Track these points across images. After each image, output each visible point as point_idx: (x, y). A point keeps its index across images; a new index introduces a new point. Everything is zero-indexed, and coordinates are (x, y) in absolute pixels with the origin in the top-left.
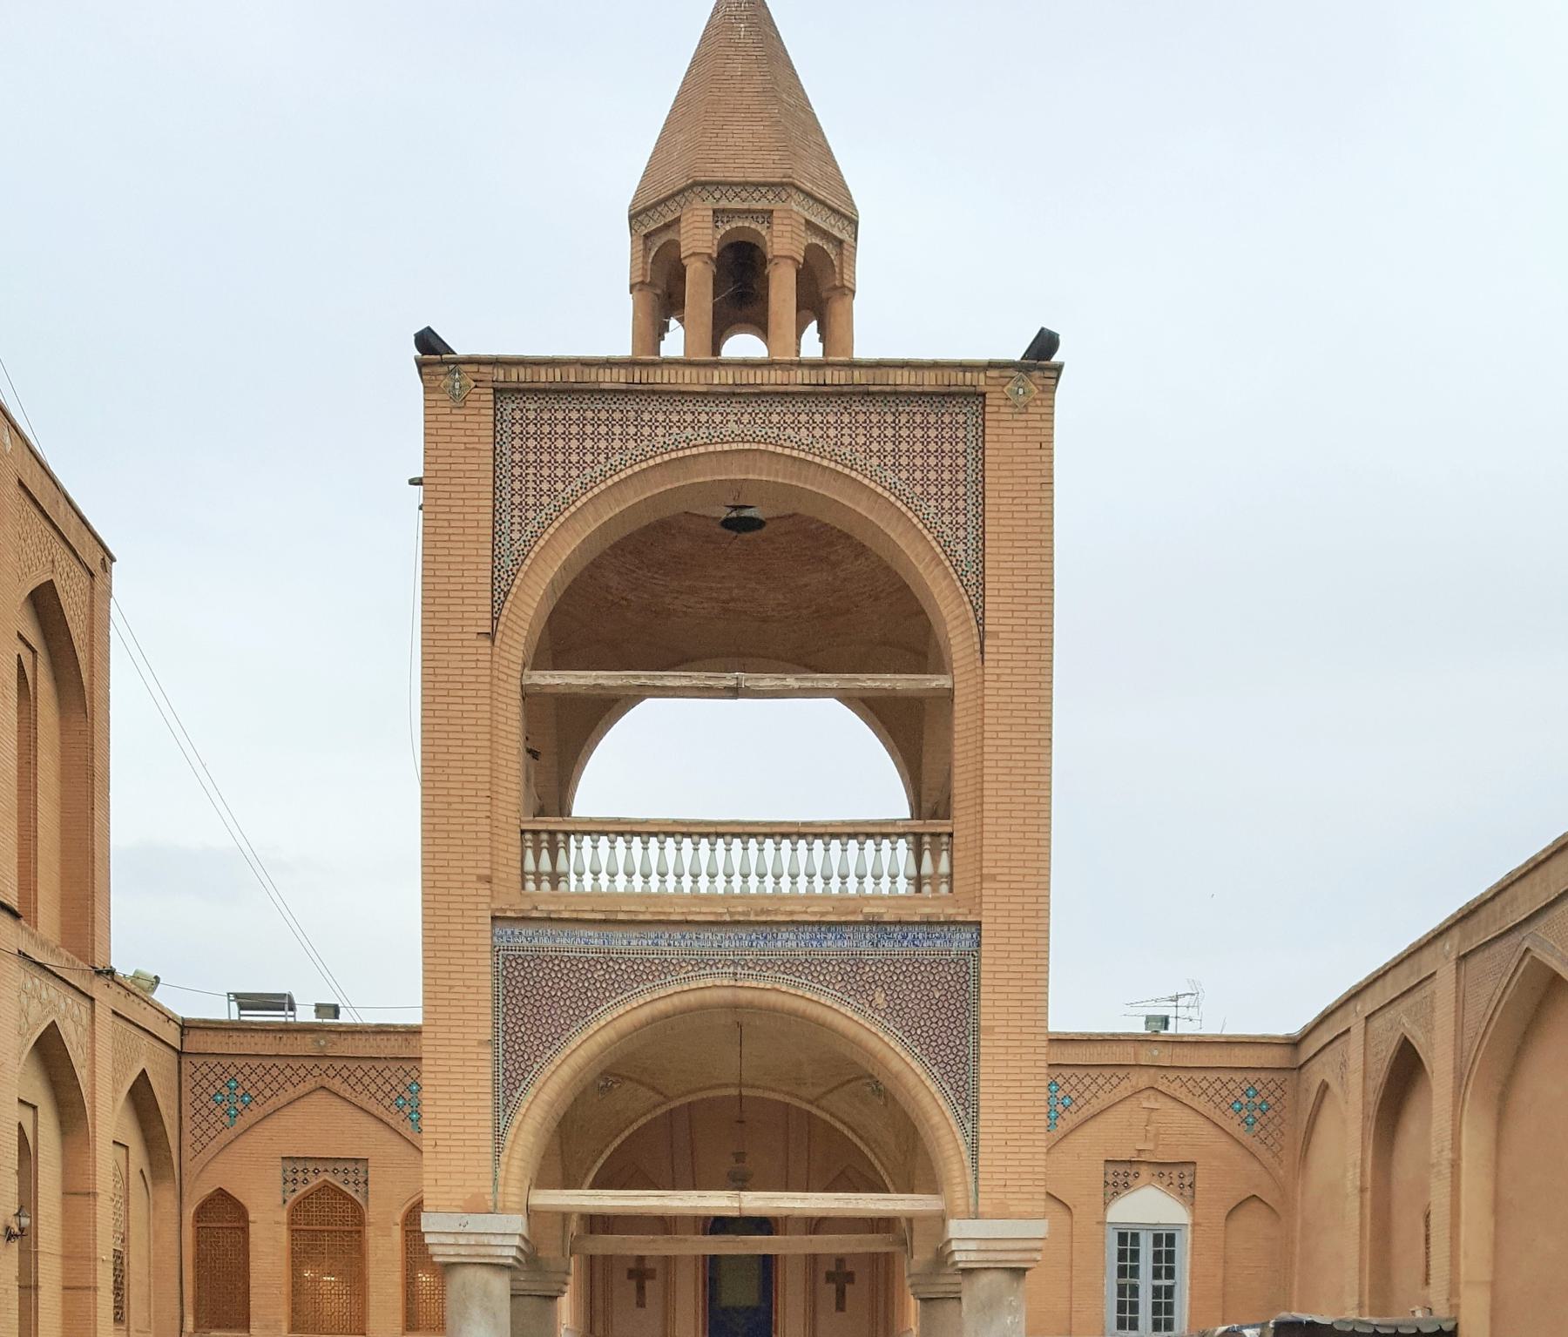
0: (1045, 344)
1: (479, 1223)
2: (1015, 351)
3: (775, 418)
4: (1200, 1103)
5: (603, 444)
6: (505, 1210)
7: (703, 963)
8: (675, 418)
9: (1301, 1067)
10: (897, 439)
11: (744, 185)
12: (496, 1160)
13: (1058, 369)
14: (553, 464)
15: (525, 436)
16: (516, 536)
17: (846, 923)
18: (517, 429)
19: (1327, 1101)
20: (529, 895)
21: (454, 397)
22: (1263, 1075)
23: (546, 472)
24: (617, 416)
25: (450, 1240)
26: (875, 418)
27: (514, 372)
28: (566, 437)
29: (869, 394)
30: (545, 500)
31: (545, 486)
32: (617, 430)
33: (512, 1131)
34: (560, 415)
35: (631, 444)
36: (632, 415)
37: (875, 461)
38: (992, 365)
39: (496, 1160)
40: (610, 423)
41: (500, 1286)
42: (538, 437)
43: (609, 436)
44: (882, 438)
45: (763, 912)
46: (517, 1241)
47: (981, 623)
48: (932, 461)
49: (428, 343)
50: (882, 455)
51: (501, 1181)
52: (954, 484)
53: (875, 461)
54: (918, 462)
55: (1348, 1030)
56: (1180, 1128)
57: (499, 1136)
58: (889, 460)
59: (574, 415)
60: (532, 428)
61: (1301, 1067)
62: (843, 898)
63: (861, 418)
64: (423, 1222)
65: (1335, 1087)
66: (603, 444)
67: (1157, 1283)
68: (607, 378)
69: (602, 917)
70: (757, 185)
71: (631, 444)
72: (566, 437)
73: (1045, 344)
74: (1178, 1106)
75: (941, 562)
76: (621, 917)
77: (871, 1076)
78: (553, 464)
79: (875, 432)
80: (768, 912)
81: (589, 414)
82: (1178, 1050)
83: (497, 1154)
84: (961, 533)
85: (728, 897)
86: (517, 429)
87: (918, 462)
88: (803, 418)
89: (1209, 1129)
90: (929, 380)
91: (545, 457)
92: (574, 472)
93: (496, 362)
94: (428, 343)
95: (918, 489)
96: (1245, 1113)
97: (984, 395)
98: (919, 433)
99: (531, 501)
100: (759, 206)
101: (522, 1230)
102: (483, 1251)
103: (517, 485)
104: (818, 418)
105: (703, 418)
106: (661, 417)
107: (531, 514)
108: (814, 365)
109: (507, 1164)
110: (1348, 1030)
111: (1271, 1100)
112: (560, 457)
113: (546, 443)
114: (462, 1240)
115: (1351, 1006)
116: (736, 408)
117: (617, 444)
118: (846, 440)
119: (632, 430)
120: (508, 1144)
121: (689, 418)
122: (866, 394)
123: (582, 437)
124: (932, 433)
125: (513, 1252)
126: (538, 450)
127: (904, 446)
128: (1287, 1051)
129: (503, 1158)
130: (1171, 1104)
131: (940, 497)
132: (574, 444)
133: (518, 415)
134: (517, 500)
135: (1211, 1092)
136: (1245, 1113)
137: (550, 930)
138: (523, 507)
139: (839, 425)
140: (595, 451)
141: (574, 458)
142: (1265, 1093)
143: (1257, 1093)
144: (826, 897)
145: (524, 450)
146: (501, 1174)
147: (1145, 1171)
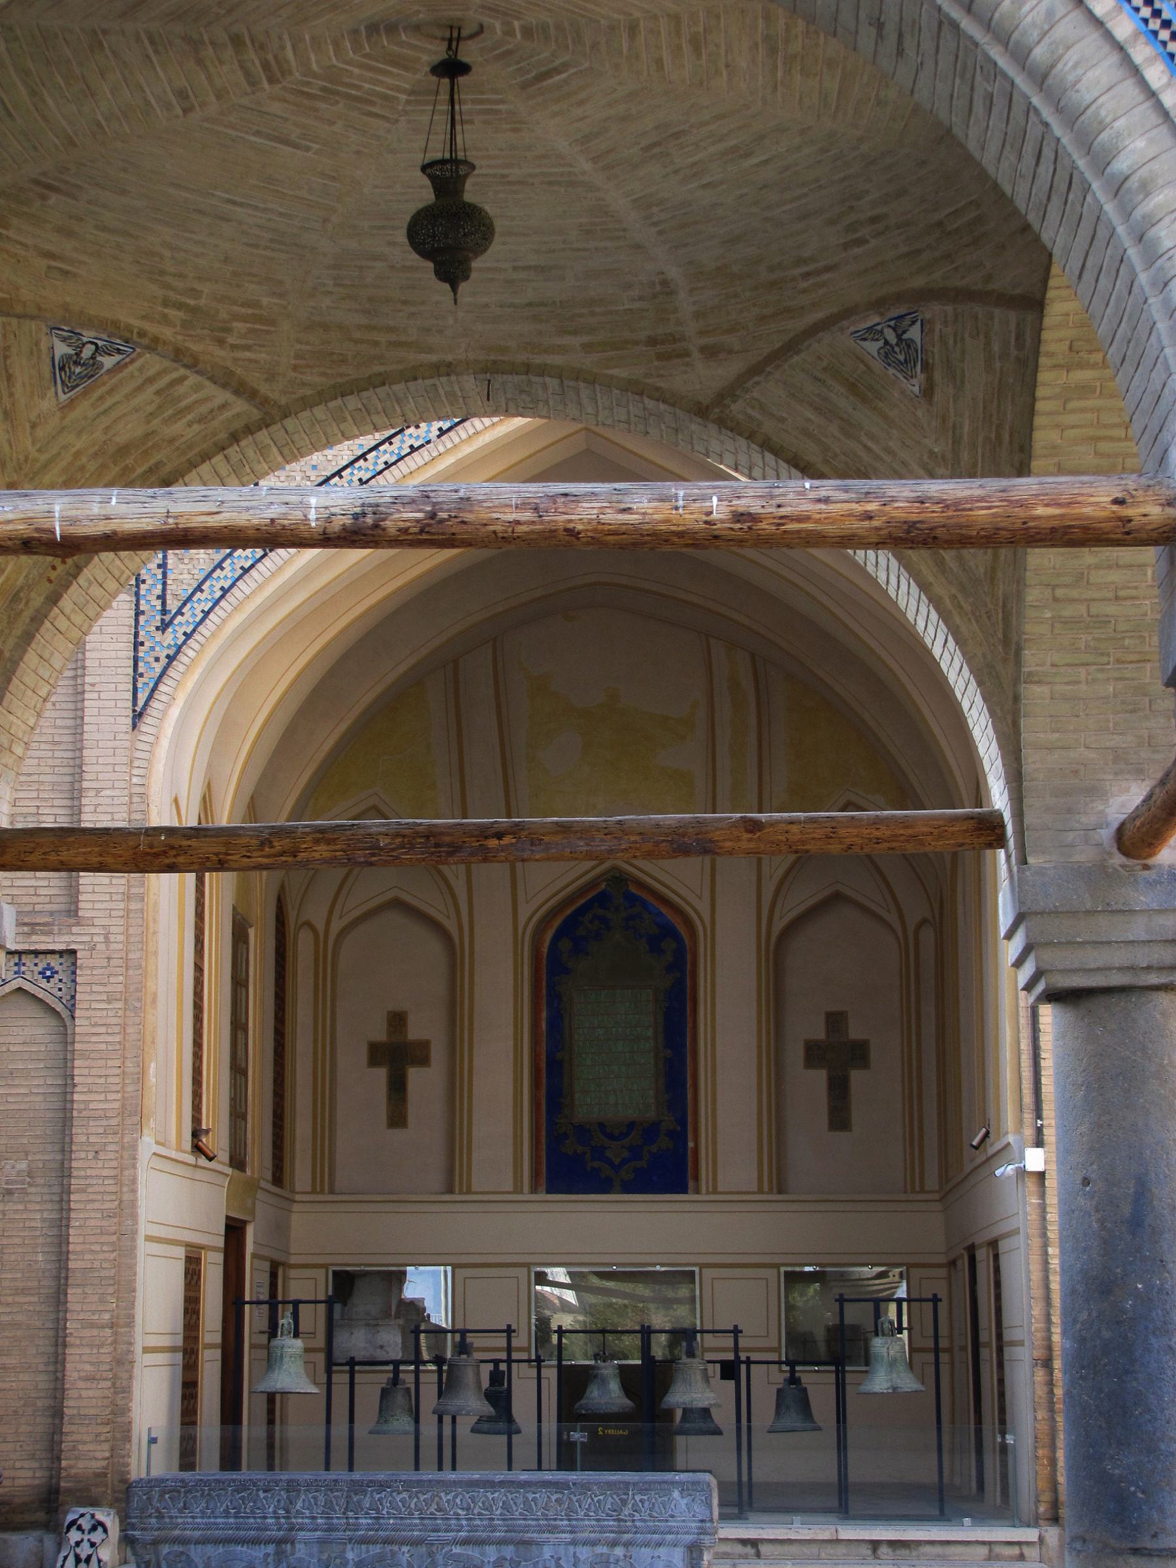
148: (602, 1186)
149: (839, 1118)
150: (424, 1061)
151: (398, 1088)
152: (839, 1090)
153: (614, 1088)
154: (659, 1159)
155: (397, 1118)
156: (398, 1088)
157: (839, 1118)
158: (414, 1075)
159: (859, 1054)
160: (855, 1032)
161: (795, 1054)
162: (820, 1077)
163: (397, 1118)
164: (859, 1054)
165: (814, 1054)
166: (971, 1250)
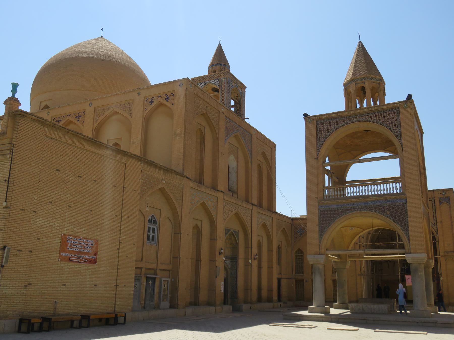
0: (410, 97)
2: (404, 99)
6: (322, 254)
10: (384, 117)
28: (328, 126)
38: (400, 102)
39: (320, 245)
43: (335, 124)
47: (402, 145)
49: (305, 115)
50: (381, 120)
52: (395, 123)
57: (320, 241)
93: (316, 116)
94: (305, 115)
108: (365, 108)
131: (392, 126)
138: (321, 138)
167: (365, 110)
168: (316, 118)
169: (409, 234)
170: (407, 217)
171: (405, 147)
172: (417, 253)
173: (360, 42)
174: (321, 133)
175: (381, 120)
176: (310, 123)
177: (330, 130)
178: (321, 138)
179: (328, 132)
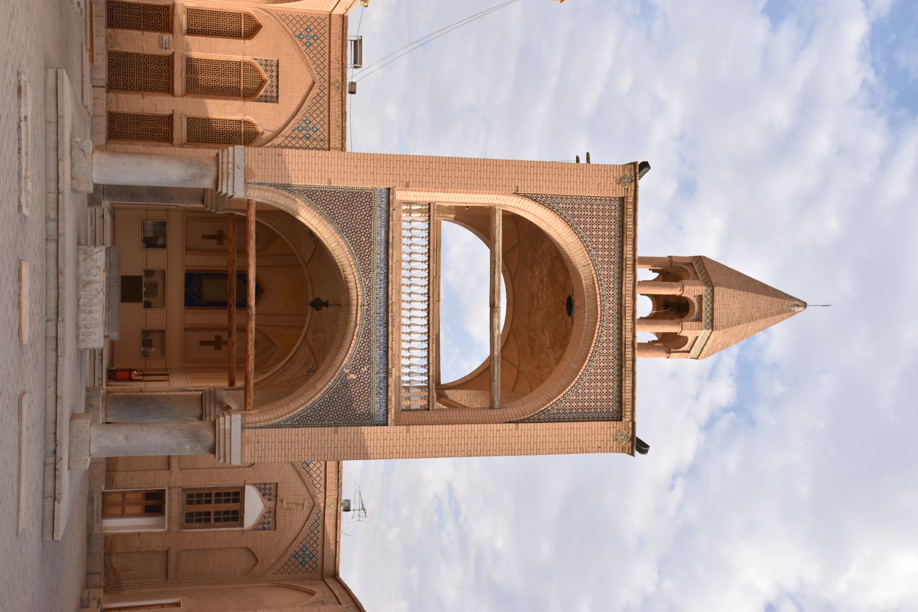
0: (641, 447)
1: (239, 174)
3: (611, 325)
4: (306, 530)
5: (600, 246)
6: (246, 188)
7: (369, 290)
8: (611, 279)
9: (323, 580)
10: (602, 381)
11: (712, 309)
12: (271, 185)
13: (633, 454)
14: (592, 223)
15: (604, 210)
16: (561, 205)
17: (387, 360)
18: (607, 207)
19: (304, 595)
20: (400, 206)
21: (621, 179)
22: (320, 558)
23: (588, 220)
24: (612, 253)
25: (230, 160)
26: (611, 371)
27: (632, 207)
28: (604, 230)
29: (621, 368)
30: (576, 219)
31: (582, 219)
32: (606, 253)
33: (287, 194)
34: (613, 227)
35: (600, 259)
36: (613, 260)
37: (593, 371)
39: (271, 185)
40: (609, 250)
41: (208, 183)
42: (604, 217)
43: (603, 249)
44: (602, 374)
45: (393, 319)
46: (230, 194)
47: (523, 421)
48: (593, 397)
49: (645, 166)
50: (596, 374)
51: (261, 187)
53: (593, 371)
54: (592, 391)
55: (340, 604)
56: (293, 521)
58: (593, 378)
59: (613, 234)
60: (607, 214)
61: (323, 580)
62: (399, 357)
63: (611, 364)
64: (240, 146)
65: (313, 599)
66: (600, 246)
67: (212, 514)
68: (628, 249)
69: (390, 241)
70: (712, 315)
71: (600, 259)
72: (604, 230)
73: (641, 447)
74: (305, 519)
75: (549, 402)
76: (390, 250)
77: (317, 368)
78: (592, 223)
79: (605, 371)
80: (392, 322)
81: (613, 240)
82: (334, 517)
83: (275, 186)
84: (561, 411)
85: (400, 301)
86: (607, 207)
87: (592, 391)
88: (611, 338)
89: (293, 535)
90: (627, 396)
91: (594, 220)
92: (588, 233)
94: (645, 166)
95: (580, 391)
96: (301, 553)
97: (621, 420)
98: (605, 391)
99: (576, 213)
100: (703, 315)
101: (236, 196)
102: (225, 176)
103: (583, 206)
104: (611, 345)
105: (611, 292)
106: (612, 273)
107: (570, 213)
109: (270, 191)
110: (340, 604)
111: (307, 566)
112: (594, 226)
113: (601, 220)
114: (230, 166)
115: (352, 604)
116: (616, 307)
117: (600, 253)
118: (602, 358)
119: (606, 260)
120: (280, 191)
121: (611, 286)
122: (621, 366)
123: (603, 237)
124: (605, 397)
125: (224, 191)
126: (598, 217)
127: (599, 384)
128: (332, 573)
129: (272, 188)
130: (306, 515)
132: (600, 233)
133: (613, 207)
134: (576, 206)
135: (312, 535)
136: (301, 553)
137: (384, 216)
138: (573, 209)
139: (608, 355)
140: (597, 243)
141: (594, 233)
142: (311, 563)
143: (311, 558)
144: (400, 349)
145: (598, 210)
146: (265, 187)
147: (272, 503)
148: (187, 285)
149: (202, 343)
150: (219, 243)
151: (212, 237)
152: (209, 343)
153: (210, 290)
154: (192, 300)
155: (204, 237)
156: (212, 237)
157: (202, 343)
158: (214, 241)
159: (218, 348)
160: (224, 347)
161: (218, 333)
162: (213, 339)
163: (204, 237)
164: (218, 348)
165: (218, 338)
166: (167, 375)
167: (629, 336)
168: (631, 200)
169: (292, 426)
170: (337, 425)
171: (517, 429)
172: (242, 446)
173: (805, 305)
174: (586, 209)
175: (596, 374)
176: (620, 181)
177: (591, 236)
178: (573, 209)
179: (585, 229)
